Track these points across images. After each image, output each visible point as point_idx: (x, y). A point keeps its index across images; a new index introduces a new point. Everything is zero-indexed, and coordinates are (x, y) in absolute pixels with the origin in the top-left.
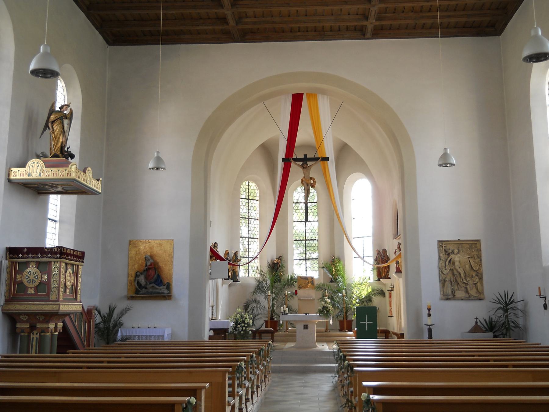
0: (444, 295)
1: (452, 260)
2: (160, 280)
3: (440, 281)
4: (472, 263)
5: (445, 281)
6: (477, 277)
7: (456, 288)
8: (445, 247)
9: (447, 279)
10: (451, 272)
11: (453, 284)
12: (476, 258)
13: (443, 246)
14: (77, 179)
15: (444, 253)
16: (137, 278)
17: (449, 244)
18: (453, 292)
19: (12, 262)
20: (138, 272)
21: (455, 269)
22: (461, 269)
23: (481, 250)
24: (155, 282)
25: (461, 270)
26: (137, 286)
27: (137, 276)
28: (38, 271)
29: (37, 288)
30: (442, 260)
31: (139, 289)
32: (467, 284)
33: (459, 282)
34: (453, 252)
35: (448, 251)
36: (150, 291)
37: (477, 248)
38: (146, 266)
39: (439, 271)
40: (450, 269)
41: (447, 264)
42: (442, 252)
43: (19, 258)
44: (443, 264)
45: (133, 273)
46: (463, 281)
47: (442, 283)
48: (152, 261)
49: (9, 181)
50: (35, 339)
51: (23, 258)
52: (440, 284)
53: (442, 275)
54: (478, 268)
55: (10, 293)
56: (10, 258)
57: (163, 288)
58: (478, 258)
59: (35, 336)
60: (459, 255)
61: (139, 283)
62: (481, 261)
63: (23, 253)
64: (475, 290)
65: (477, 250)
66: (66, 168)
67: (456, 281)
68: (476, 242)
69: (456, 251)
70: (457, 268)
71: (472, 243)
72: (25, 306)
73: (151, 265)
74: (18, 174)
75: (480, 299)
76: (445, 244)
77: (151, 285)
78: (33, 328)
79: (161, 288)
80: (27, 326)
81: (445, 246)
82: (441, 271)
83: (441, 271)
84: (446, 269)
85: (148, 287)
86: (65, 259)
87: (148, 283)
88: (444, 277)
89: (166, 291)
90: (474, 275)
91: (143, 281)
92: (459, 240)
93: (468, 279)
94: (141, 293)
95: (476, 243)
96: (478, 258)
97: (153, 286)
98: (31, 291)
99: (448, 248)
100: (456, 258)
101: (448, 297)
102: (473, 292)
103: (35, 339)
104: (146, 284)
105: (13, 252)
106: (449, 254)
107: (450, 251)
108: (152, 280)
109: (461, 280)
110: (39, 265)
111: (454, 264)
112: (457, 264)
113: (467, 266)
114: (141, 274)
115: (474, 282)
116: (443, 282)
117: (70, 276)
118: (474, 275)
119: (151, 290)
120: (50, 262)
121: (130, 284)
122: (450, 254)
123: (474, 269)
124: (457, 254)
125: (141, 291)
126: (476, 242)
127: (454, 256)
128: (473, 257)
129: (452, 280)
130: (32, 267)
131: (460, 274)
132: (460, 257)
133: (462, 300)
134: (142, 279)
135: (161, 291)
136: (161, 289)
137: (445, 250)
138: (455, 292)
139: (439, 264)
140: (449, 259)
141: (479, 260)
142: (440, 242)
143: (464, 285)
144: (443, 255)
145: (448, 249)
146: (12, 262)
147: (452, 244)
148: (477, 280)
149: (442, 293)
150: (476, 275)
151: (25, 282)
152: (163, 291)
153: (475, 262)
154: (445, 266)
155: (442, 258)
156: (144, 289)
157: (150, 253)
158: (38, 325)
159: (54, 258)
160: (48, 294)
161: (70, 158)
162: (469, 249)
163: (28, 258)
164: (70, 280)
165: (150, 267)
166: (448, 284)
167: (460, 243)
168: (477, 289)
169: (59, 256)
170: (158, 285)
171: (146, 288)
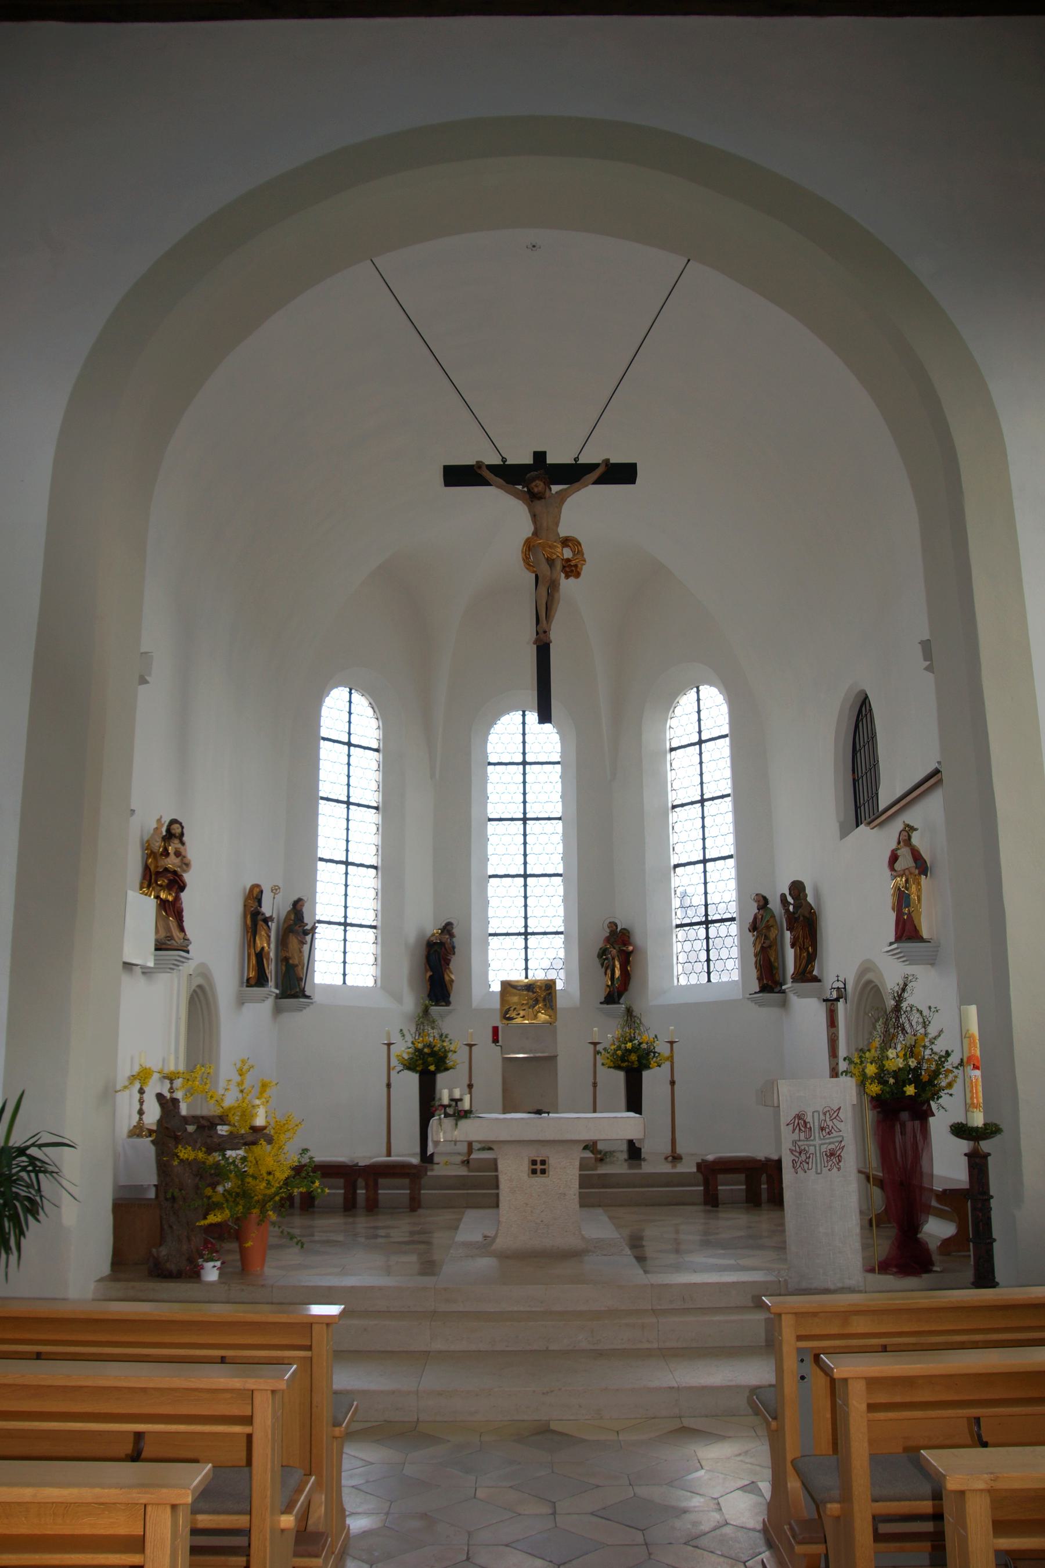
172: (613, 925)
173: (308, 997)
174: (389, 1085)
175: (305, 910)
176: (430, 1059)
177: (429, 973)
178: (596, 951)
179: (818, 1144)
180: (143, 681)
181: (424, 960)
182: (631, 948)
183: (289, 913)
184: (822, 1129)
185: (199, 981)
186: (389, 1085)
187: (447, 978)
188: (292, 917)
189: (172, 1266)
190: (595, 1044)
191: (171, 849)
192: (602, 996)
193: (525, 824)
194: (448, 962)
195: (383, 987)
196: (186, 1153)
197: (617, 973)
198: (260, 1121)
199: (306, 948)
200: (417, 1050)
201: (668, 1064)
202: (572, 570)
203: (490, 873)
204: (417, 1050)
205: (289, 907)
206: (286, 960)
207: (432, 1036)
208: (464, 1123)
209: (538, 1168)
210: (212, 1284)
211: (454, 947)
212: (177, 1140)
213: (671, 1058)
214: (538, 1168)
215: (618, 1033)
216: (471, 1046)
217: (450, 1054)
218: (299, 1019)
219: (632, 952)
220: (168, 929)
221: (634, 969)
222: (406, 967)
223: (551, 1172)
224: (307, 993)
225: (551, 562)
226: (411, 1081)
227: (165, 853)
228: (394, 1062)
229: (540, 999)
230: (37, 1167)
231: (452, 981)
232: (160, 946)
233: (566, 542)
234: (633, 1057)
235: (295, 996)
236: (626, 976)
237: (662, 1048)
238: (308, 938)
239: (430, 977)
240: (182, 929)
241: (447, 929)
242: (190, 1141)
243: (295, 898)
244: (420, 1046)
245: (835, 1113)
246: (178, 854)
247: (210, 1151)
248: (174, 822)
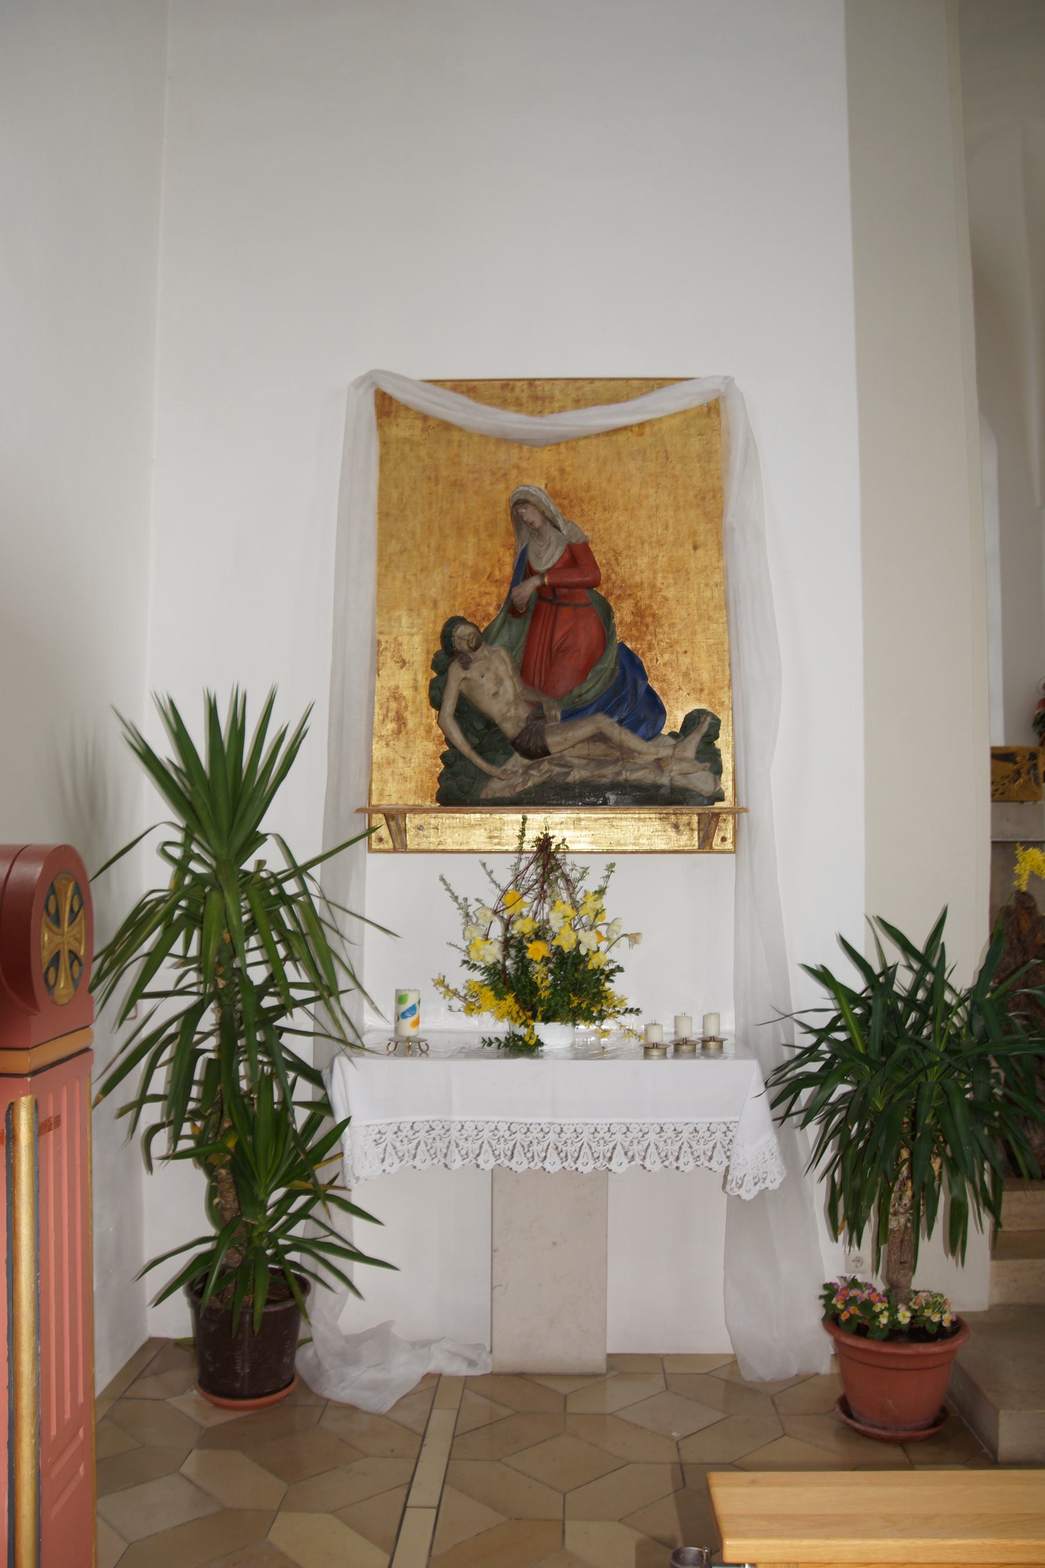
2: (641, 690)
16: (456, 672)
20: (461, 620)
24: (607, 705)
31: (479, 761)
36: (555, 772)
38: (523, 570)
77: (585, 729)
85: (554, 741)
94: (496, 787)
97: (600, 737)
104: (538, 715)
108: (593, 687)
121: (391, 726)
125: (489, 777)
135: (664, 780)
152: (685, 774)
156: (517, 761)
157: (550, 479)
171: (537, 752)
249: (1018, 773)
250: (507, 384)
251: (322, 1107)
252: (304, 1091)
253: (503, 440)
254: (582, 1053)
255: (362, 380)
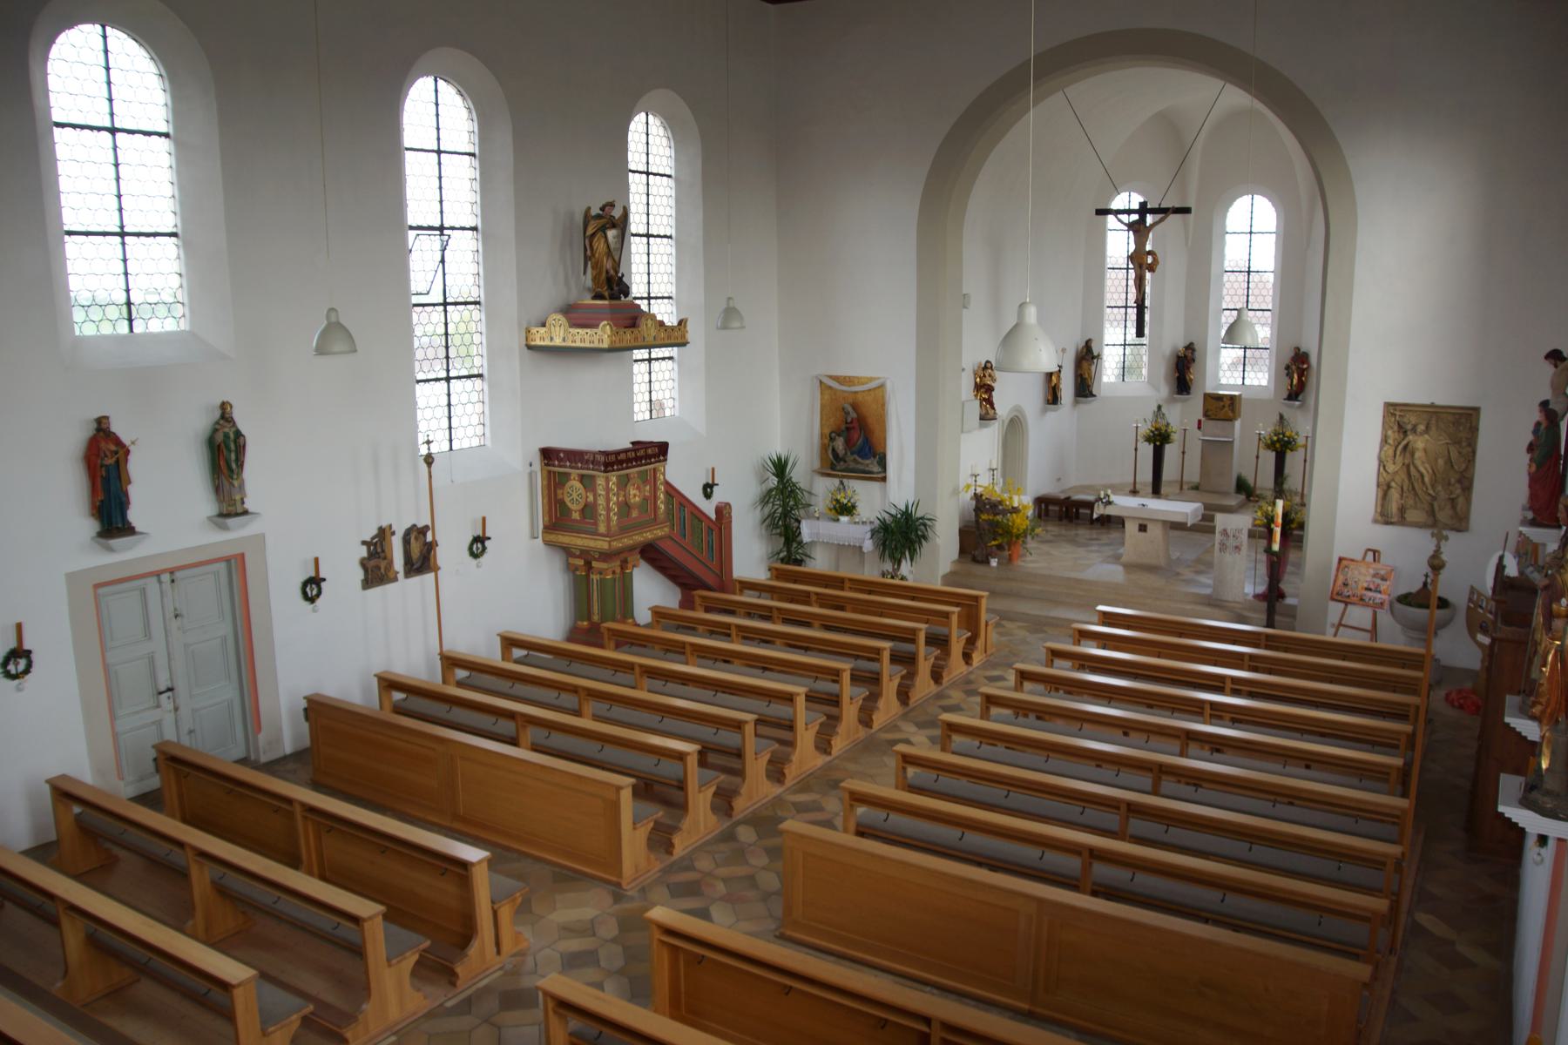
0: (1382, 514)
1: (1410, 446)
2: (867, 449)
3: (1378, 486)
4: (1454, 454)
5: (1389, 487)
6: (1458, 485)
7: (1411, 502)
8: (1400, 416)
9: (1393, 484)
10: (1405, 469)
11: (1404, 494)
12: (1464, 444)
13: (1395, 415)
14: (618, 345)
15: (1396, 428)
17: (1410, 411)
18: (1402, 510)
19: (549, 472)
21: (1413, 463)
22: (1427, 466)
23: (1477, 430)
25: (1426, 469)
26: (831, 456)
27: (832, 439)
28: (582, 486)
29: (582, 511)
30: (1389, 444)
31: (835, 462)
32: (1434, 498)
33: (1419, 492)
34: (1414, 430)
35: (1404, 426)
36: (851, 467)
37: (1471, 423)
39: (1379, 465)
40: (1403, 464)
41: (1398, 453)
42: (1392, 428)
43: (554, 466)
44: (1391, 452)
45: (827, 431)
46: (1427, 489)
47: (1383, 490)
48: (854, 415)
49: (530, 347)
50: (595, 581)
51: (560, 466)
52: (1377, 491)
53: (1385, 474)
54: (1464, 466)
55: (550, 517)
56: (545, 464)
57: (872, 463)
58: (1469, 445)
59: (595, 577)
60: (1426, 436)
61: (833, 450)
62: (1474, 452)
63: (560, 460)
64: (1448, 511)
65: (1471, 428)
66: (595, 330)
67: (1414, 489)
68: (1470, 412)
69: (1421, 428)
70: (1418, 463)
71: (1460, 414)
72: (567, 537)
73: (851, 422)
74: (540, 337)
75: (1459, 531)
76: (1401, 411)
77: (852, 458)
78: (588, 565)
79: (868, 462)
80: (581, 562)
81: (1402, 414)
82: (1384, 467)
83: (1382, 464)
84: (1394, 463)
85: (847, 459)
86: (613, 470)
87: (849, 453)
88: (1388, 478)
89: (876, 469)
90: (1453, 481)
91: (841, 448)
92: (1432, 405)
93: (1439, 488)
94: (838, 468)
95: (1471, 415)
96: (1469, 445)
97: (855, 459)
98: (576, 516)
99: (1405, 420)
100: (1419, 443)
101: (1390, 520)
102: (1443, 516)
103: (595, 581)
104: (846, 454)
105: (548, 454)
106: (1405, 433)
107: (1409, 427)
109: (1425, 489)
110: (582, 478)
111: (1412, 454)
112: (1417, 455)
113: (1441, 462)
114: (839, 435)
115: (1451, 493)
116: (1384, 489)
117: (638, 488)
118: (1453, 481)
119: (852, 465)
120: (593, 477)
122: (1409, 433)
123: (1456, 467)
124: (1421, 434)
126: (1470, 412)
127: (1416, 438)
128: (1457, 442)
129: (1405, 488)
130: (574, 479)
131: (1422, 476)
132: (1427, 440)
133: (1421, 527)
134: (840, 444)
135: (867, 469)
136: (867, 465)
137: (1399, 424)
138: (1408, 511)
139: (1380, 451)
140: (1404, 443)
141: (1470, 449)
142: (1388, 405)
143: (1428, 498)
144: (1394, 432)
145: (1404, 423)
146: (549, 472)
147: (1416, 411)
148: (1459, 491)
149: (1379, 510)
150: (1459, 481)
151: (567, 500)
153: (1460, 453)
154: (1395, 456)
155: (1391, 441)
156: (842, 463)
158: (594, 564)
159: (597, 470)
160: (596, 524)
161: (623, 298)
162: (1454, 424)
163: (565, 467)
164: (638, 494)
165: (851, 426)
166: (1394, 494)
167: (1434, 415)
168: (1454, 507)
169: (603, 468)
170: (862, 457)
171: (845, 462)
172: (1298, 349)
173: (1094, 396)
174: (1136, 449)
175: (1093, 345)
176: (1158, 438)
177: (1177, 375)
178: (1284, 366)
179: (1231, 542)
180: (965, 307)
181: (1174, 366)
182: (1305, 366)
183: (1083, 348)
184: (1234, 536)
185: (1015, 413)
186: (1136, 449)
187: (1188, 378)
188: (1085, 350)
189: (979, 558)
190: (1260, 434)
191: (987, 375)
192: (1285, 397)
193: (1249, 275)
194: (1188, 368)
195: (1148, 382)
196: (984, 517)
197: (1295, 381)
198: (1016, 505)
199: (1093, 368)
200: (1152, 431)
201: (1303, 450)
202: (1151, 268)
203: (1224, 307)
204: (1152, 431)
205: (1084, 344)
206: (1081, 375)
207: (1162, 423)
208: (1109, 507)
209: (1143, 528)
210: (993, 567)
211: (1194, 361)
212: (982, 512)
213: (1305, 446)
214: (1143, 528)
215: (1273, 428)
216: (1185, 430)
217: (1172, 434)
218: (1088, 406)
219: (1304, 370)
220: (986, 409)
221: (1312, 380)
222: (1163, 369)
223: (1148, 530)
224: (1094, 393)
225: (1141, 266)
226: (1147, 450)
227: (984, 376)
228: (1139, 437)
229: (1227, 405)
230: (925, 525)
231: (1191, 380)
232: (982, 418)
233: (1149, 253)
234: (1278, 445)
235: (1086, 396)
236: (1302, 386)
237: (1301, 441)
238: (1095, 361)
239: (1178, 378)
240: (994, 409)
241: (1190, 347)
242: (988, 512)
243: (1087, 338)
244: (1153, 429)
245: (1240, 531)
246: (990, 376)
247: (996, 514)
248: (988, 362)
249: (1224, 406)
250: (845, 377)
251: (799, 528)
252: (796, 524)
253: (843, 391)
254: (850, 523)
255: (816, 377)
